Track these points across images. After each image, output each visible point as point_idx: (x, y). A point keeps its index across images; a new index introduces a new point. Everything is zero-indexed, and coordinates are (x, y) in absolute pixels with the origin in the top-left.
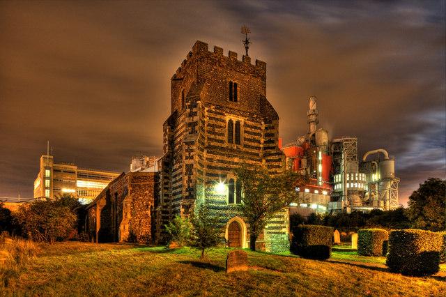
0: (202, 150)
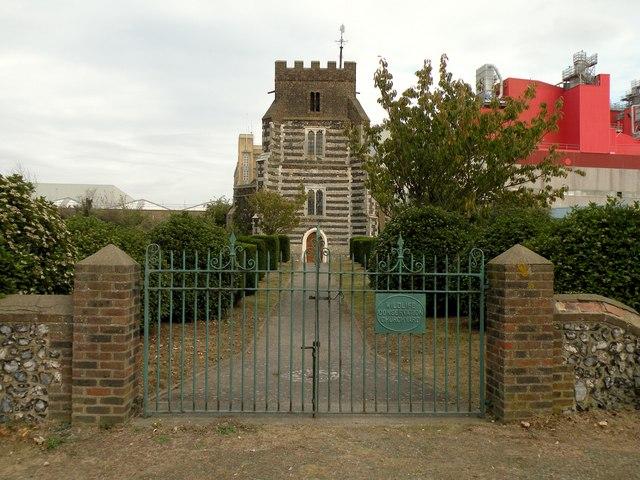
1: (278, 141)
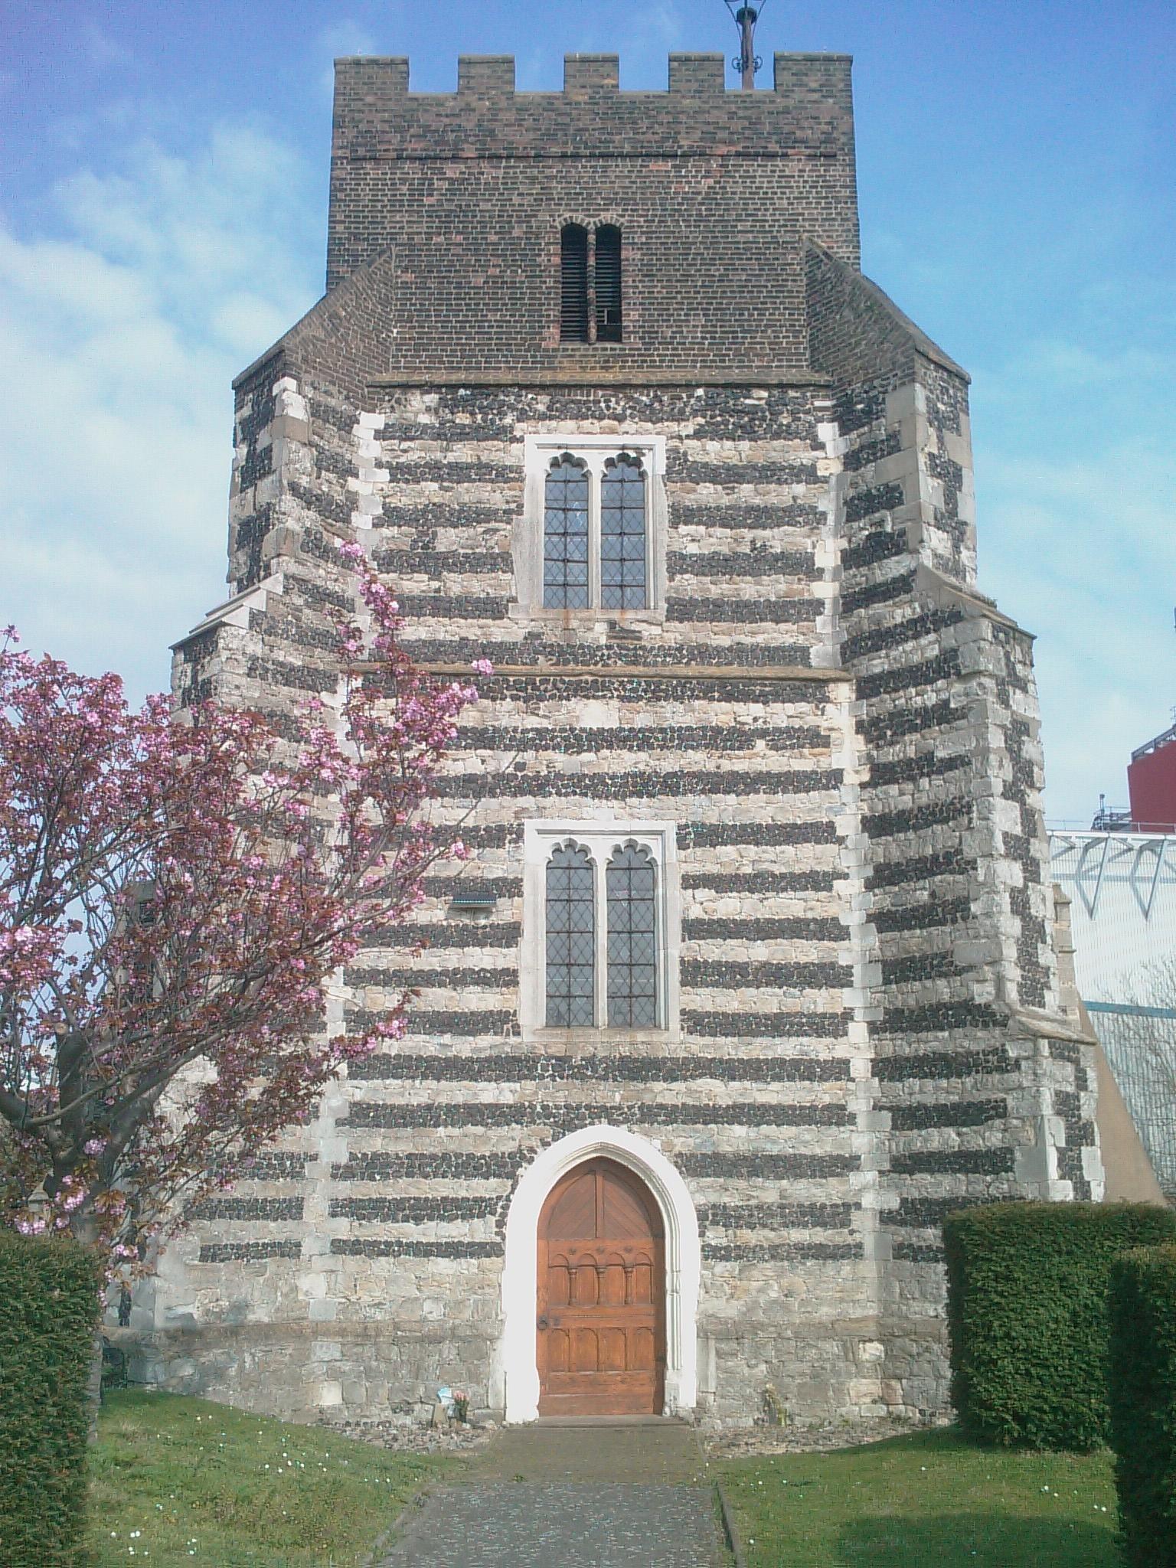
0: (316, 681)
1: (339, 512)
